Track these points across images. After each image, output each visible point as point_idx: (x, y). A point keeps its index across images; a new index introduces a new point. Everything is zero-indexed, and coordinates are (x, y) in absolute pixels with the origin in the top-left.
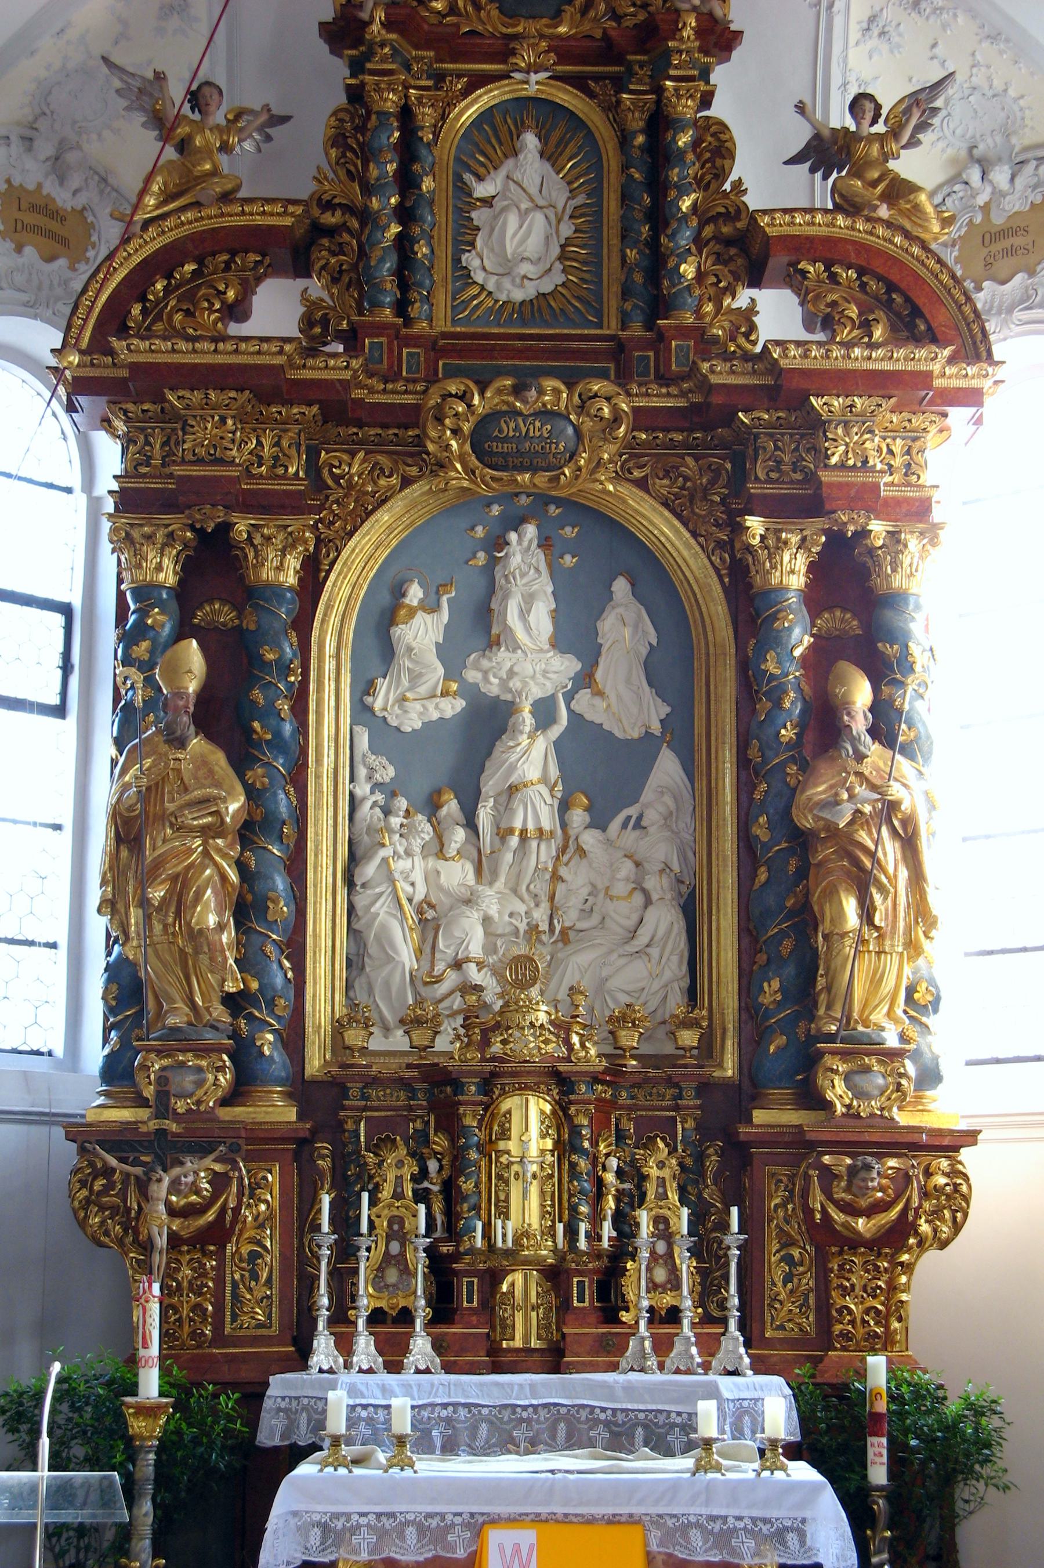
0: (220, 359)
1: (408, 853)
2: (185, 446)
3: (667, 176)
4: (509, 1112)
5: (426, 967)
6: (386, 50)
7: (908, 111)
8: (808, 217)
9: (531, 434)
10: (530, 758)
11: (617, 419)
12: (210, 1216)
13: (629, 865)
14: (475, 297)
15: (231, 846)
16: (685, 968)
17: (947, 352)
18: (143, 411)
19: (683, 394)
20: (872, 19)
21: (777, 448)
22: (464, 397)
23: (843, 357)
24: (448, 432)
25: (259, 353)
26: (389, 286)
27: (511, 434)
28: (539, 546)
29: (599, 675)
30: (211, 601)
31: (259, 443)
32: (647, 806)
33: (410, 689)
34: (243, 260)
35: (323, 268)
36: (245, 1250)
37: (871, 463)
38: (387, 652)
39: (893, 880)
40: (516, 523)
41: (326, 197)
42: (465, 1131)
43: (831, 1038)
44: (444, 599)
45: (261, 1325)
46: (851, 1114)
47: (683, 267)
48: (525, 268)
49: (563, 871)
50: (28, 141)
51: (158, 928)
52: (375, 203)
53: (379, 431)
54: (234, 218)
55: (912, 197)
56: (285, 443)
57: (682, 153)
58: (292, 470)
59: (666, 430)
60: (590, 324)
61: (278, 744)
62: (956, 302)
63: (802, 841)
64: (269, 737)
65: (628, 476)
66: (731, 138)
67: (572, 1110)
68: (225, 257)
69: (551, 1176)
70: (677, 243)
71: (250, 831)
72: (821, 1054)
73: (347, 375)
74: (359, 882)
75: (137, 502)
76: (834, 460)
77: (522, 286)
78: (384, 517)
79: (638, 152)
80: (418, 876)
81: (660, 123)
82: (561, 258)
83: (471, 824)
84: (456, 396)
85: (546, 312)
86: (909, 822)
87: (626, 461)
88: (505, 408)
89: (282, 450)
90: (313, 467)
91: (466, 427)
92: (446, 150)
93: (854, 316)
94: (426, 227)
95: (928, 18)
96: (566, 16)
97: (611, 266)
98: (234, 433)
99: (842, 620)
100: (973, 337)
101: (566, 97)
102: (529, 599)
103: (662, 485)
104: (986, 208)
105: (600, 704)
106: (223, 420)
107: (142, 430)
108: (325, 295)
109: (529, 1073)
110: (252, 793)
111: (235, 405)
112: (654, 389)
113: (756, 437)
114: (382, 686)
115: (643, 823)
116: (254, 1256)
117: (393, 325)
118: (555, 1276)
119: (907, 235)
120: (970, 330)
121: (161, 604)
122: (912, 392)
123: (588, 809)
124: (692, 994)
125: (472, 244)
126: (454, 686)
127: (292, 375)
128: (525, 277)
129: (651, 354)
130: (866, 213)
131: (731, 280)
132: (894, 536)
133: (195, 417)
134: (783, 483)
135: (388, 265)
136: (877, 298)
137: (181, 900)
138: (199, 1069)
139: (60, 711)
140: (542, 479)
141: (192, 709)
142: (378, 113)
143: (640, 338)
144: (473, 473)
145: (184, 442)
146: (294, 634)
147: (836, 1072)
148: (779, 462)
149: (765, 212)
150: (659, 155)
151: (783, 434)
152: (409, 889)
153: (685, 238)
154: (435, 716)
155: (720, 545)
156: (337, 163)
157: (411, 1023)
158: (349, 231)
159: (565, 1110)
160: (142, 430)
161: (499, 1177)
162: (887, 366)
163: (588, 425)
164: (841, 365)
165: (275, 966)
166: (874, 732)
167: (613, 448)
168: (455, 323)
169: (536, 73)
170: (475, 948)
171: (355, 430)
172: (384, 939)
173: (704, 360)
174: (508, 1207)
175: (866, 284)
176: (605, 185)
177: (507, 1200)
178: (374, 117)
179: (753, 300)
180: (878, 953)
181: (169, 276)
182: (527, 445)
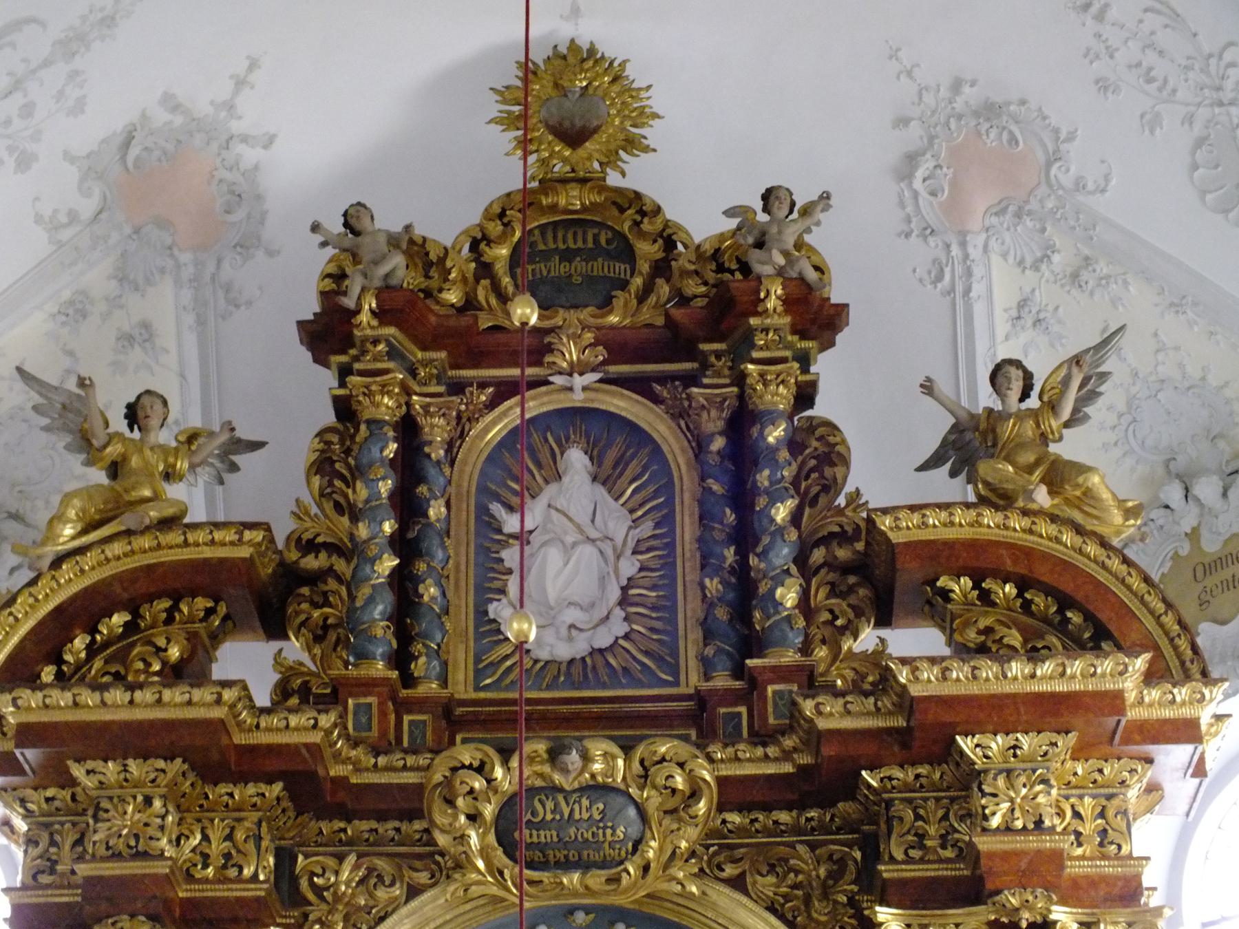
0: (139, 715)
2: (96, 838)
3: (755, 482)
6: (381, 347)
7: (1066, 382)
8: (944, 515)
9: (577, 816)
11: (694, 795)
14: (507, 657)
17: (1140, 663)
18: (48, 800)
19: (786, 756)
20: (1023, 304)
21: (918, 817)
22: (481, 769)
23: (997, 678)
24: (462, 819)
25: (190, 703)
26: (380, 633)
27: (549, 817)
31: (206, 838)
34: (190, 608)
35: (303, 624)
37: (1047, 823)
41: (306, 536)
47: (779, 592)
48: (572, 615)
52: (363, 531)
53: (374, 824)
54: (172, 550)
55: (1080, 480)
56: (240, 835)
57: (774, 450)
58: (247, 872)
59: (767, 808)
60: (666, 683)
62: (1152, 612)
65: (716, 872)
66: (844, 442)
68: (166, 604)
70: (769, 562)
73: (316, 738)
76: (995, 822)
77: (570, 639)
79: (717, 459)
81: (743, 420)
82: (624, 602)
84: (470, 767)
85: (602, 671)
87: (715, 854)
88: (539, 783)
89: (234, 846)
91: (489, 811)
93: (1017, 645)
94: (436, 564)
95: (1092, 294)
96: (618, 303)
98: (163, 817)
100: (1179, 655)
101: (622, 404)
103: (766, 884)
104: (1193, 536)
106: (148, 801)
107: (47, 826)
108: (305, 658)
111: (163, 780)
112: (744, 750)
113: (889, 804)
117: (386, 680)
119: (1079, 530)
120: (1175, 648)
125: (502, 591)
127: (239, 739)
128: (572, 626)
129: (743, 710)
130: (1020, 503)
131: (851, 615)
133: (111, 798)
134: (929, 862)
135: (380, 608)
136: (1046, 620)
140: (596, 879)
142: (369, 422)
143: (728, 691)
144: (501, 873)
145: (95, 831)
148: (922, 836)
149: (885, 511)
150: (742, 451)
151: (925, 799)
153: (783, 554)
156: (322, 495)
158: (339, 579)
160: (47, 826)
162: (1060, 687)
163: (652, 799)
168: (477, 688)
169: (581, 374)
171: (342, 825)
173: (806, 697)
175: (1031, 601)
176: (678, 508)
178: (363, 427)
179: (882, 640)
181: (93, 631)
182: (572, 831)
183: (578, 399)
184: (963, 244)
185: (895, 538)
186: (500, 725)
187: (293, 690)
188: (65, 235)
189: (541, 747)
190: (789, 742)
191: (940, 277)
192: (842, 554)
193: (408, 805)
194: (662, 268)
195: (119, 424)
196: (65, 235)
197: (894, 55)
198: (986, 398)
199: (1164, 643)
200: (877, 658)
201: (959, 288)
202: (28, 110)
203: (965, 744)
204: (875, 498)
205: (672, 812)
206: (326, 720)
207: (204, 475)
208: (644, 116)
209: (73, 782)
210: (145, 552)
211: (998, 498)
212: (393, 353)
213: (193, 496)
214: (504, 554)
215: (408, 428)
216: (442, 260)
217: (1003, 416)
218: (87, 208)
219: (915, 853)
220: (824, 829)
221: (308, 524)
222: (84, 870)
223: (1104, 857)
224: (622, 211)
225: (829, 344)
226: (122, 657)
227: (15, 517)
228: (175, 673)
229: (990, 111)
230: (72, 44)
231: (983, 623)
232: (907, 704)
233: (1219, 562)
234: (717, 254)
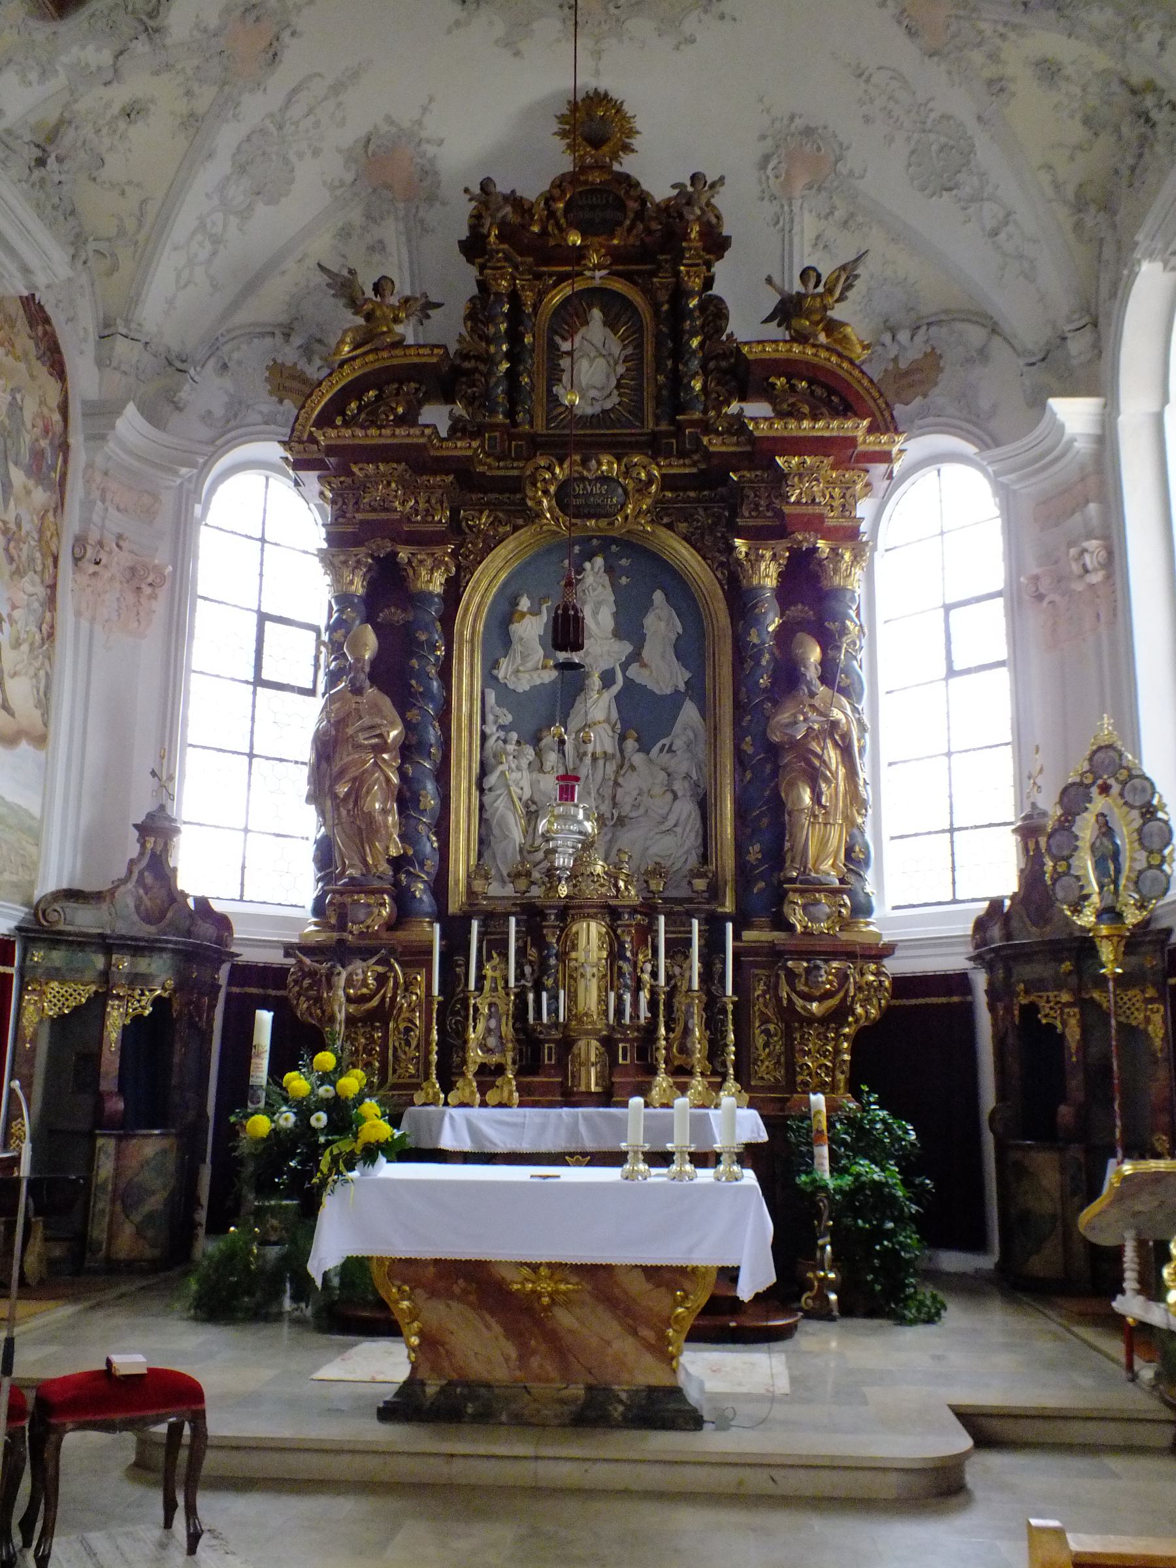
0: (382, 441)
1: (519, 769)
4: (577, 933)
5: (530, 842)
7: (838, 277)
10: (598, 706)
11: (650, 482)
12: (375, 1002)
13: (663, 775)
14: (561, 414)
15: (394, 759)
16: (700, 840)
17: (865, 423)
18: (341, 483)
19: (694, 464)
20: (818, 237)
21: (756, 496)
22: (550, 468)
26: (500, 400)
28: (605, 571)
29: (645, 654)
30: (388, 607)
31: (417, 502)
32: (677, 736)
33: (521, 665)
36: (402, 1026)
38: (507, 642)
42: (548, 946)
43: (792, 881)
44: (544, 608)
45: (411, 1076)
46: (807, 933)
48: (593, 393)
49: (620, 780)
50: (287, 336)
51: (344, 812)
52: (492, 349)
54: (398, 359)
56: (433, 501)
57: (692, 311)
59: (685, 489)
61: (427, 694)
62: (873, 397)
63: (773, 751)
64: (421, 690)
67: (619, 931)
68: (396, 386)
69: (606, 975)
71: (408, 750)
72: (786, 892)
73: (470, 453)
74: (486, 786)
76: (793, 499)
78: (502, 552)
81: (679, 294)
82: (618, 386)
86: (846, 736)
91: (552, 489)
97: (649, 391)
99: (802, 611)
100: (885, 420)
102: (598, 605)
103: (683, 527)
105: (645, 672)
106: (389, 484)
107: (341, 495)
108: (464, 413)
109: (591, 907)
110: (408, 726)
111: (396, 473)
114: (504, 662)
115: (674, 748)
116: (408, 1030)
117: (503, 425)
118: (608, 1043)
119: (840, 355)
120: (883, 415)
121: (352, 605)
122: (842, 452)
123: (638, 740)
124: (704, 858)
125: (560, 380)
126: (552, 663)
127: (433, 453)
130: (811, 341)
132: (834, 550)
136: (820, 399)
137: (357, 794)
138: (369, 905)
139: (312, 692)
140: (603, 523)
141: (367, 669)
143: (666, 431)
146: (438, 623)
147: (796, 903)
148: (757, 505)
149: (746, 343)
150: (678, 312)
152: (519, 791)
153: (695, 364)
154: (538, 682)
155: (722, 565)
157: (515, 876)
158: (481, 373)
159: (615, 932)
161: (571, 977)
162: (827, 434)
163: (630, 484)
164: (795, 434)
165: (425, 839)
166: (823, 679)
167: (649, 501)
168: (548, 428)
172: (502, 823)
174: (576, 996)
177: (576, 991)
180: (825, 824)
181: (360, 399)
183: (597, 283)
184: (790, 205)
185: (750, 357)
186: (559, 448)
187: (458, 428)
188: (338, 192)
189: (577, 458)
190: (696, 457)
191: (777, 222)
192: (724, 364)
193: (515, 486)
194: (640, 215)
195: (370, 293)
196: (338, 192)
197: (761, 100)
198: (797, 287)
199: (878, 414)
200: (740, 415)
201: (787, 228)
202: (317, 124)
203: (780, 461)
204: (741, 336)
205: (638, 491)
206: (475, 444)
207: (413, 320)
208: (632, 133)
209: (353, 474)
210: (385, 359)
211: (801, 338)
212: (507, 258)
213: (407, 330)
214: (561, 362)
215: (514, 297)
216: (530, 209)
217: (805, 296)
218: (349, 177)
219: (753, 514)
220: (712, 500)
221: (465, 345)
222: (359, 516)
223: (844, 517)
224: (620, 184)
225: (720, 257)
226: (374, 413)
227: (320, 341)
228: (401, 421)
229: (808, 132)
230: (337, 88)
231: (791, 400)
232: (752, 439)
233: (907, 373)
234: (668, 207)
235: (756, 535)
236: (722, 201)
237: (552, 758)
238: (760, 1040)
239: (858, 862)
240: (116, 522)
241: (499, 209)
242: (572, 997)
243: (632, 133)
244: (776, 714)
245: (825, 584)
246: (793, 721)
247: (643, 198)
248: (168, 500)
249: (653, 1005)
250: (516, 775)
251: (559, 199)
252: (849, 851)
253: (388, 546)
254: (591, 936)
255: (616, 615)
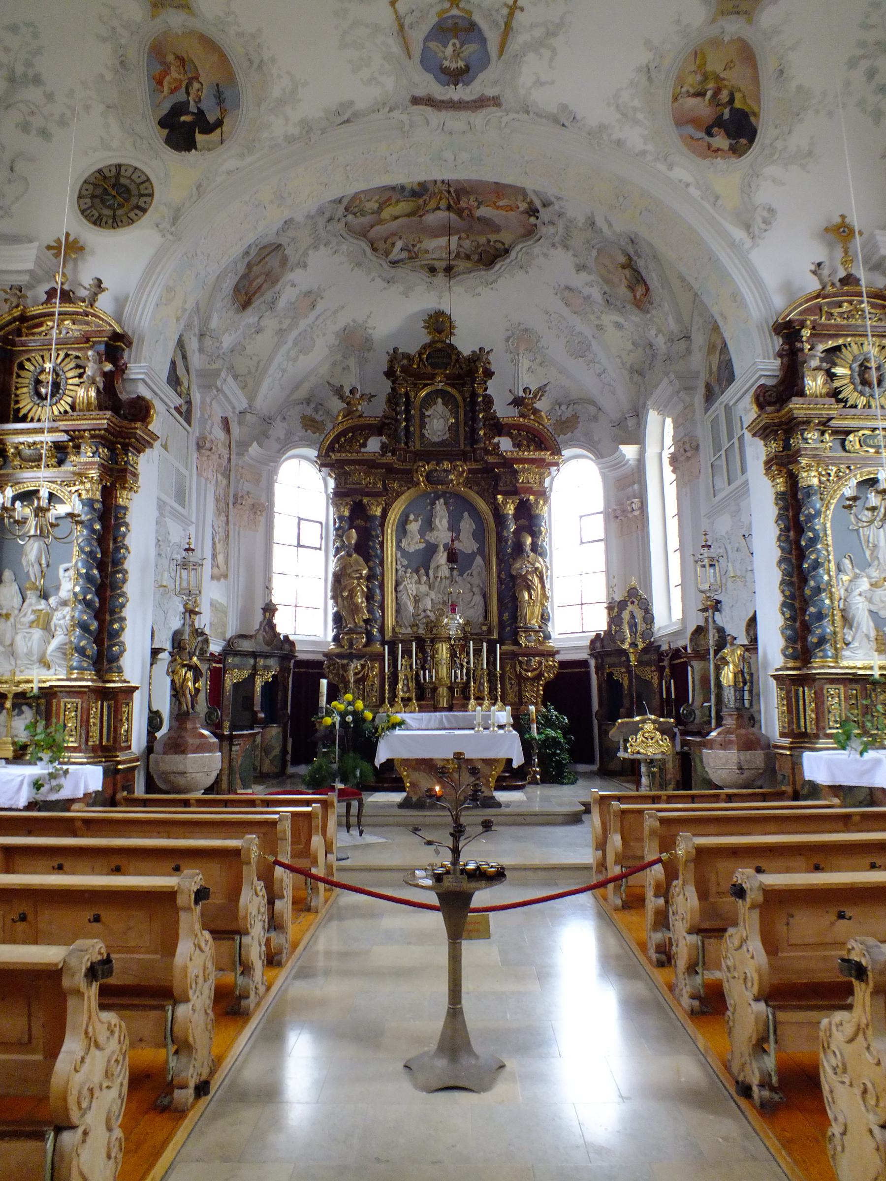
10: (441, 558)
11: (463, 471)
29: (460, 537)
38: (405, 532)
39: (537, 587)
40: (438, 499)
42: (427, 653)
48: (439, 433)
61: (376, 556)
63: (513, 578)
71: (370, 578)
75: (339, 495)
78: (403, 497)
80: (414, 589)
81: (474, 395)
83: (428, 575)
90: (384, 485)
92: (418, 402)
97: (462, 432)
101: (449, 389)
103: (476, 488)
110: (370, 568)
114: (404, 540)
118: (451, 689)
124: (486, 618)
132: (536, 500)
137: (352, 596)
139: (320, 549)
140: (444, 487)
150: (473, 403)
153: (481, 424)
157: (412, 626)
166: (532, 550)
170: (429, 607)
183: (440, 387)
187: (384, 448)
193: (409, 472)
194: (457, 361)
197: (507, 317)
198: (521, 394)
208: (455, 327)
210: (357, 422)
211: (523, 416)
215: (407, 395)
217: (525, 398)
234: (469, 359)
235: (506, 494)
236: (491, 357)
237: (425, 578)
238: (508, 687)
239: (545, 620)
240: (247, 487)
241: (401, 361)
242: (437, 673)
243: (455, 327)
244: (513, 564)
245: (533, 513)
246: (522, 567)
247: (459, 354)
248: (264, 474)
249: (468, 674)
250: (410, 586)
251: (423, 354)
252: (542, 615)
253: (360, 498)
254: (443, 651)
255: (448, 522)
